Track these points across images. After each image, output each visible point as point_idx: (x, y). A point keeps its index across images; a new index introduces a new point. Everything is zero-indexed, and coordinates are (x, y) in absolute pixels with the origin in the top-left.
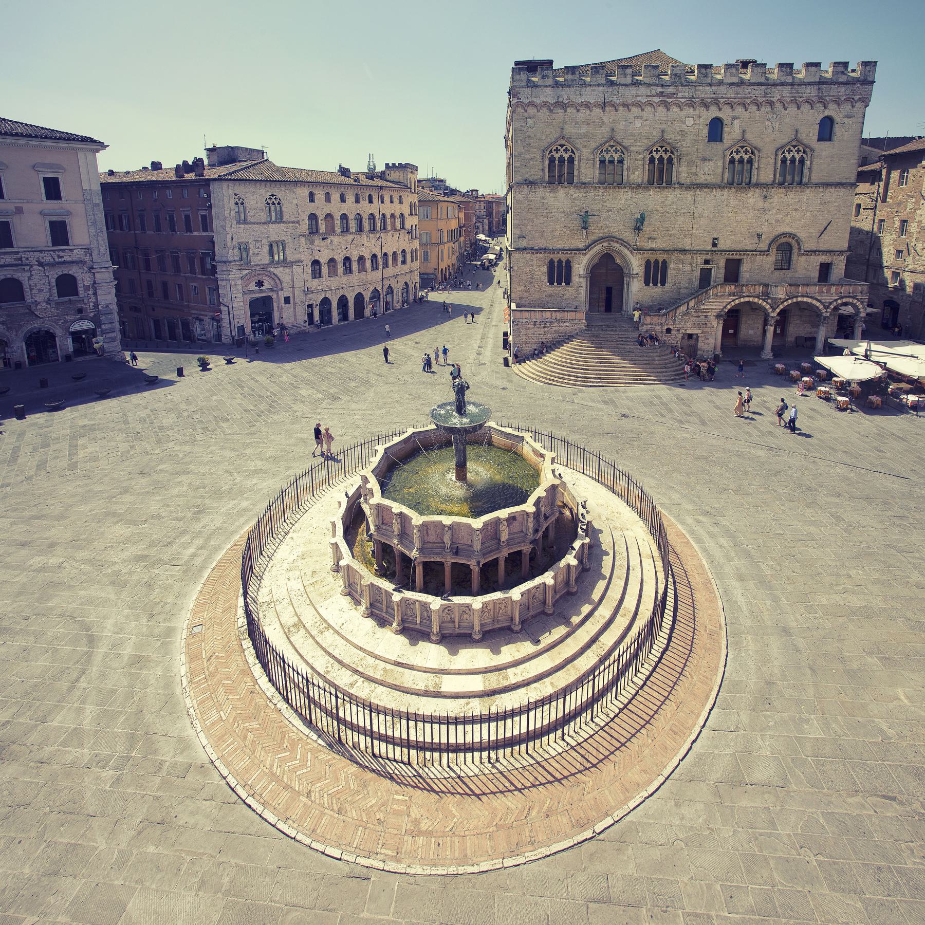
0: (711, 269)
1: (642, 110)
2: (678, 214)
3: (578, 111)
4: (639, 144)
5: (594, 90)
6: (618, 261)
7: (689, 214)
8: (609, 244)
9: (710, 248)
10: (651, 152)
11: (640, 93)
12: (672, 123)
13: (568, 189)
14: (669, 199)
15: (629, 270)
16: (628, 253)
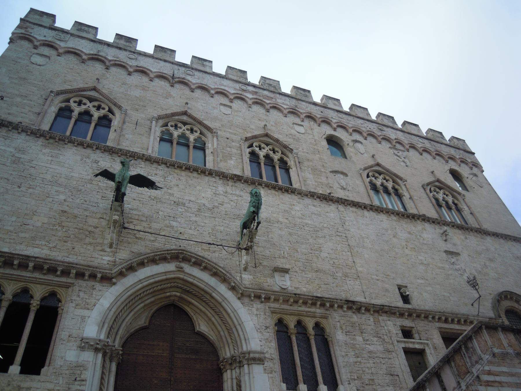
0: (421, 353)
1: (231, 101)
2: (320, 234)
3: (130, 74)
4: (229, 130)
5: (159, 63)
6: (202, 327)
7: (338, 238)
8: (180, 269)
9: (400, 303)
10: (251, 146)
11: (225, 84)
12: (276, 124)
13: (89, 151)
14: (297, 208)
15: (236, 343)
16: (229, 295)
